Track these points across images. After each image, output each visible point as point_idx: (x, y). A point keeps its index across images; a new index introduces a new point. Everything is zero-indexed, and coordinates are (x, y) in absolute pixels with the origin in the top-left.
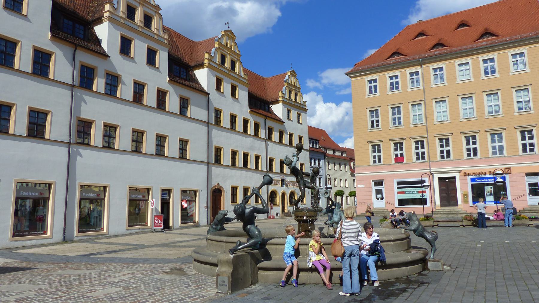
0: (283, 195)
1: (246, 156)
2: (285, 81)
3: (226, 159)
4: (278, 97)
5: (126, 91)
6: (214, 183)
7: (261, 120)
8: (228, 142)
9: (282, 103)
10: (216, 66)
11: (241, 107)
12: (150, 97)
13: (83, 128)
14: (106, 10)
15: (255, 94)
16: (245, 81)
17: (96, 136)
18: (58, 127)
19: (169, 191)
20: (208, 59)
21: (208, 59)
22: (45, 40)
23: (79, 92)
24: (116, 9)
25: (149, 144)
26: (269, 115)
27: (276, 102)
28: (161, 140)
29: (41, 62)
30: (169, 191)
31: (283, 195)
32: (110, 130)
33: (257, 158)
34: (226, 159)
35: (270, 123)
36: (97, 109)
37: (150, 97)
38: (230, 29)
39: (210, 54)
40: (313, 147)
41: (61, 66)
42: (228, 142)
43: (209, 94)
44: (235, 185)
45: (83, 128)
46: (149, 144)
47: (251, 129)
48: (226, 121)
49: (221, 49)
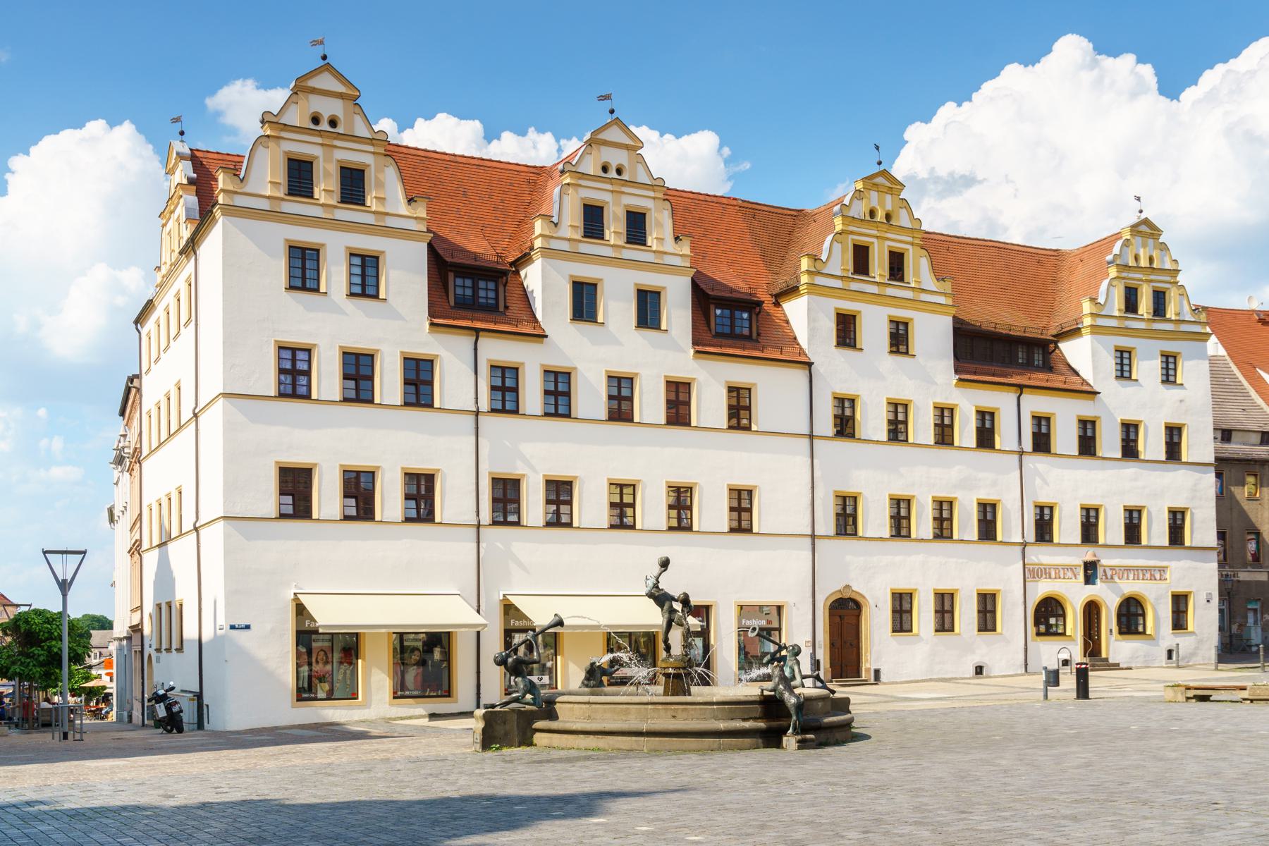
0: (1092, 610)
2: (1109, 263)
3: (874, 519)
4: (1078, 320)
5: (591, 396)
6: (829, 589)
7: (1001, 401)
8: (875, 475)
9: (1092, 333)
10: (838, 284)
11: (930, 377)
12: (650, 403)
13: (506, 494)
14: (538, 230)
15: (991, 328)
16: (942, 300)
17: (534, 505)
18: (458, 498)
20: (809, 272)
21: (809, 272)
22: (419, 336)
23: (493, 424)
24: (556, 225)
26: (1039, 378)
27: (1075, 332)
29: (419, 381)
32: (560, 492)
34: (874, 519)
35: (1035, 403)
36: (534, 450)
37: (650, 403)
38: (882, 167)
39: (815, 259)
41: (457, 381)
42: (875, 475)
43: (810, 364)
44: (903, 586)
45: (506, 494)
47: (966, 432)
48: (873, 422)
49: (852, 233)
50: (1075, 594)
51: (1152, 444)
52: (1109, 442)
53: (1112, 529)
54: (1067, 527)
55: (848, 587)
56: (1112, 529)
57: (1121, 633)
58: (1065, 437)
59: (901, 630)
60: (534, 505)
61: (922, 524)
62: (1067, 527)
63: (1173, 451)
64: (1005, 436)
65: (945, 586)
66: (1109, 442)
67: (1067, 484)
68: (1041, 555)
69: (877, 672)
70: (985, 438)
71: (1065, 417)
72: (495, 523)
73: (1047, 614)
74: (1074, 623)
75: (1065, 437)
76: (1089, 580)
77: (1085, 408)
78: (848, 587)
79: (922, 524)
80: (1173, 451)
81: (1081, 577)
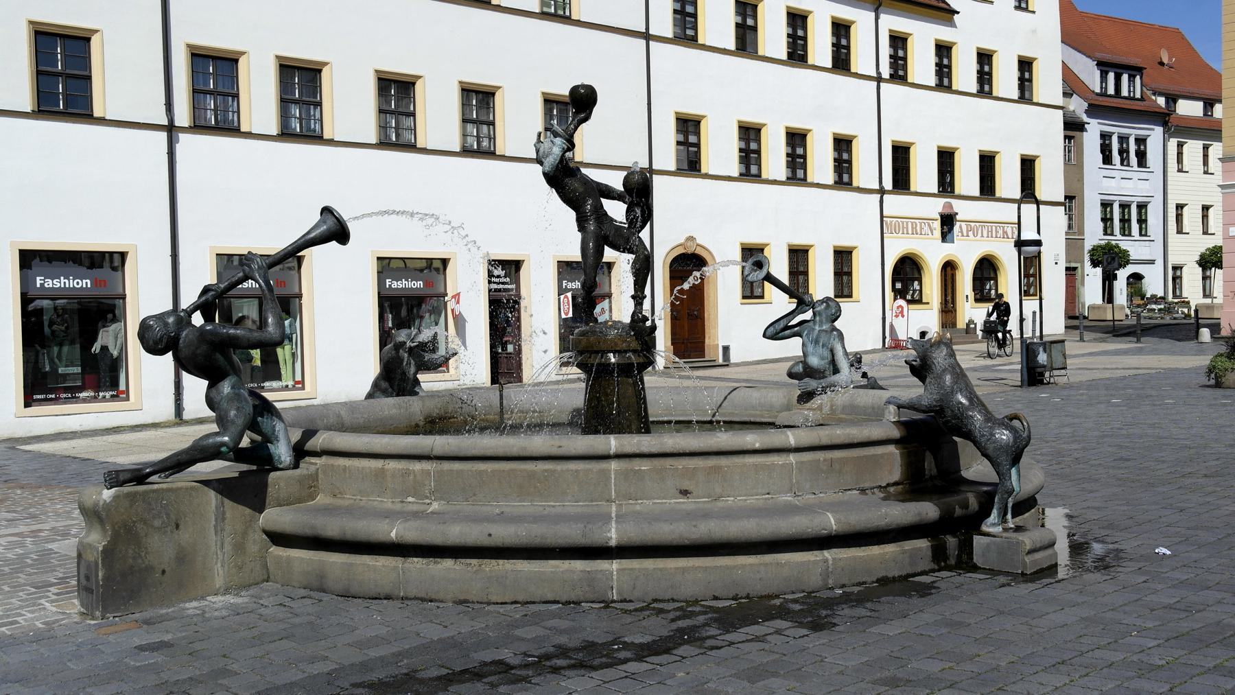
0: (949, 268)
1: (796, 139)
3: (721, 151)
17: (259, 99)
19: (513, 267)
25: (438, 117)
28: (478, 101)
30: (513, 267)
31: (949, 268)
33: (843, 144)
40: (1104, 94)
46: (438, 117)
50: (933, 253)
51: (1005, 79)
52: (965, 72)
53: (967, 177)
54: (924, 172)
55: (691, 239)
56: (967, 177)
57: (977, 300)
58: (922, 65)
59: (752, 297)
60: (259, 99)
61: (774, 159)
62: (924, 172)
63: (1025, 92)
64: (863, 57)
65: (799, 240)
66: (965, 72)
67: (927, 120)
68: (896, 204)
69: (726, 349)
70: (841, 62)
71: (923, 35)
72: (198, 127)
73: (906, 273)
74: (932, 285)
75: (922, 65)
76: (947, 234)
77: (944, 33)
78: (691, 239)
79: (774, 159)
80: (1025, 92)
81: (938, 233)
